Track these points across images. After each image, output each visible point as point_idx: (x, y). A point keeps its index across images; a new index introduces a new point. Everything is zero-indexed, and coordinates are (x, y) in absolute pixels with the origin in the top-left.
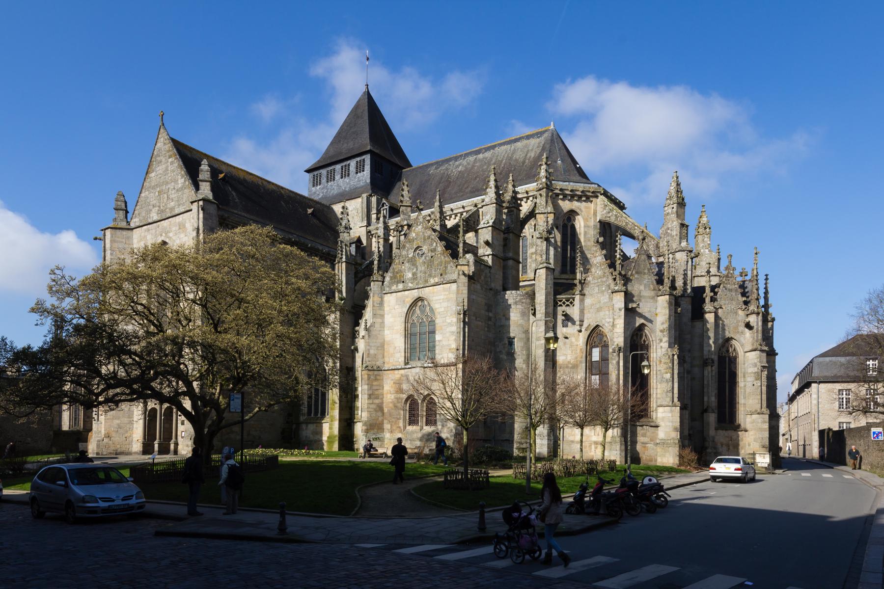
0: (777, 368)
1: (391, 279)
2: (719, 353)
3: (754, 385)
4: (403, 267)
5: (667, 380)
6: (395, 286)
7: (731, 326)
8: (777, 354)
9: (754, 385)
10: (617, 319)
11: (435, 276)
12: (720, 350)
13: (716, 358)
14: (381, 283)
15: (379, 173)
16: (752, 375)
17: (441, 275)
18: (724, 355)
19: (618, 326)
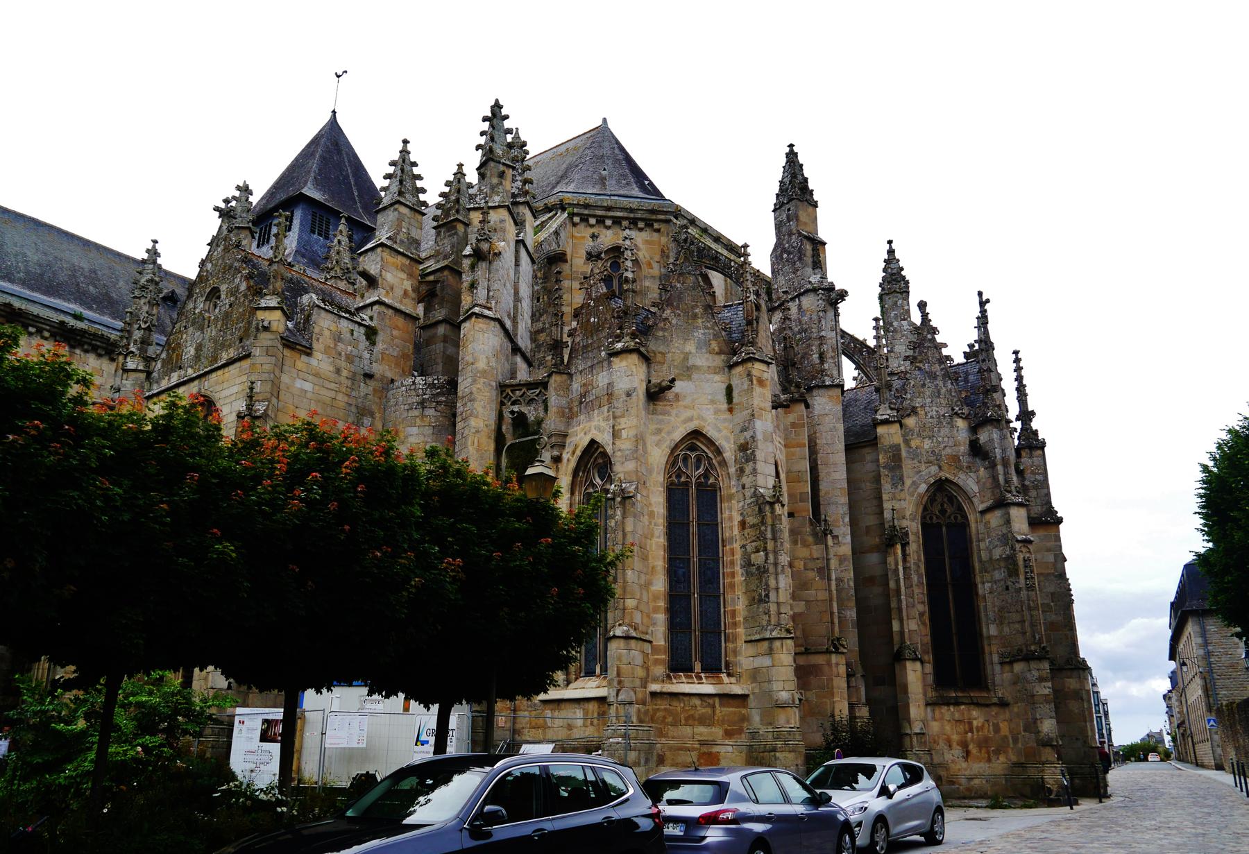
0: (1065, 551)
1: (163, 366)
2: (923, 517)
3: (1007, 588)
4: (184, 336)
5: (758, 569)
6: (167, 378)
7: (943, 453)
8: (1060, 520)
9: (1007, 588)
10: (623, 416)
11: (230, 346)
12: (925, 509)
13: (913, 527)
14: (143, 376)
15: (320, 235)
16: (1002, 564)
17: (241, 340)
18: (935, 520)
19: (624, 434)
